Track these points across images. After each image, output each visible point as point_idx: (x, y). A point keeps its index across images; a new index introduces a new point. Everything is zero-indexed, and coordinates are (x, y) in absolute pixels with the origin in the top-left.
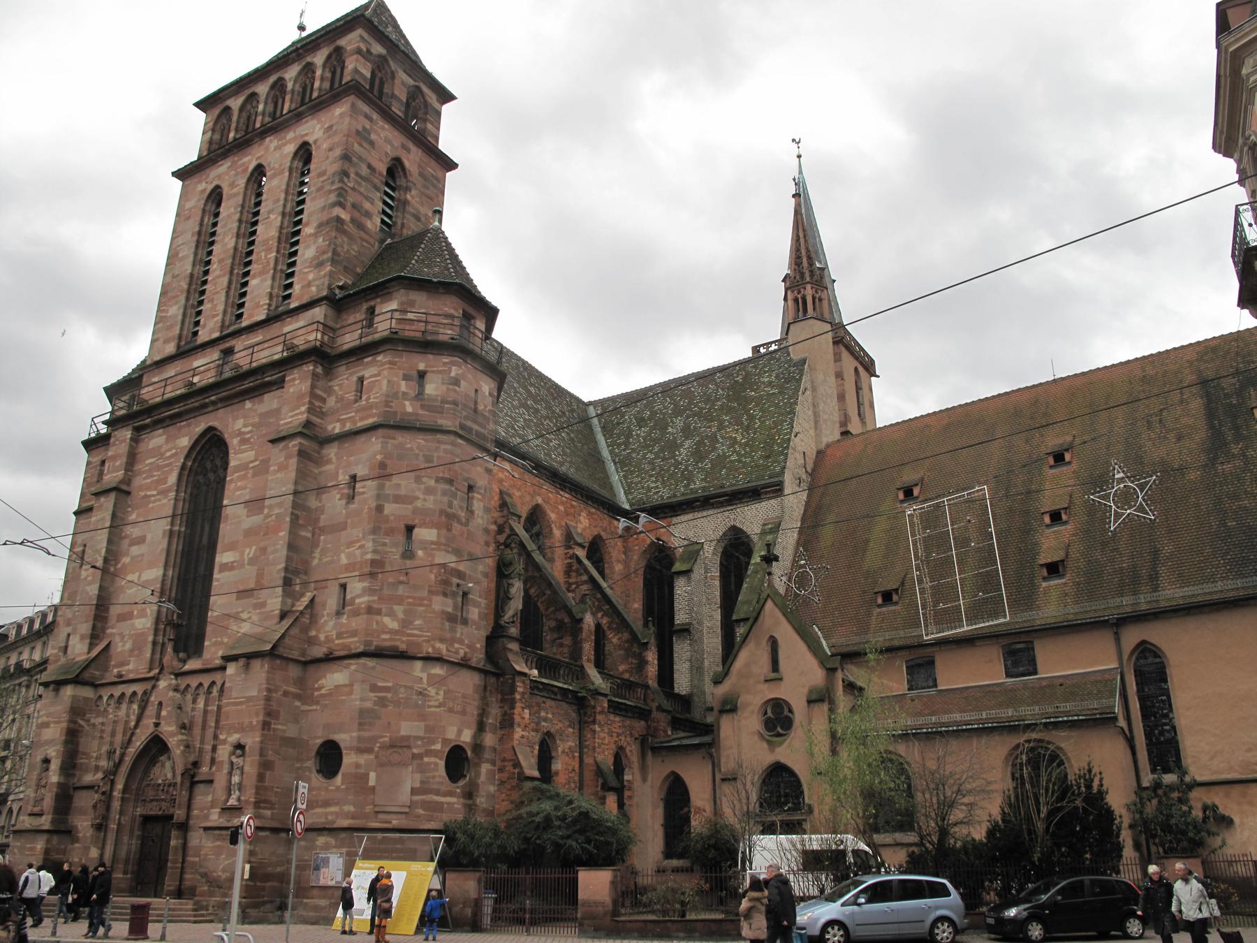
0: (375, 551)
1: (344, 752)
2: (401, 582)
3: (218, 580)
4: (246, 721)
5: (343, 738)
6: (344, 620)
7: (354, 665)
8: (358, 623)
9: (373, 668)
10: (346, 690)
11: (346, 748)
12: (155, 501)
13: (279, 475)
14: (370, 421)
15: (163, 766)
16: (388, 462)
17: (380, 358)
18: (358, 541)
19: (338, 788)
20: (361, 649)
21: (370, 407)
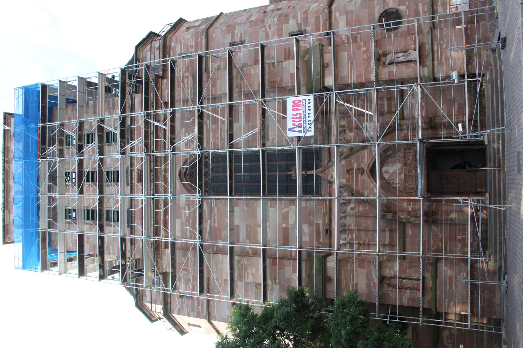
0: (274, 18)
1: (386, 8)
2: (294, 7)
3: (273, 139)
4: (364, 56)
5: (378, 11)
6: (308, 29)
7: (336, 14)
8: (312, 20)
9: (338, 4)
10: (349, 15)
11: (384, 7)
12: (214, 222)
13: (218, 85)
14: (204, 41)
15: (391, 175)
16: (228, 25)
17: (173, 44)
18: (266, 30)
19: (408, 7)
20: (327, 11)
21: (196, 43)
